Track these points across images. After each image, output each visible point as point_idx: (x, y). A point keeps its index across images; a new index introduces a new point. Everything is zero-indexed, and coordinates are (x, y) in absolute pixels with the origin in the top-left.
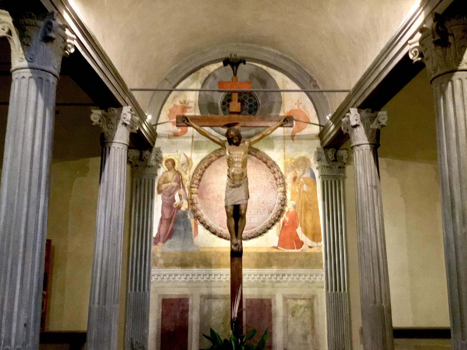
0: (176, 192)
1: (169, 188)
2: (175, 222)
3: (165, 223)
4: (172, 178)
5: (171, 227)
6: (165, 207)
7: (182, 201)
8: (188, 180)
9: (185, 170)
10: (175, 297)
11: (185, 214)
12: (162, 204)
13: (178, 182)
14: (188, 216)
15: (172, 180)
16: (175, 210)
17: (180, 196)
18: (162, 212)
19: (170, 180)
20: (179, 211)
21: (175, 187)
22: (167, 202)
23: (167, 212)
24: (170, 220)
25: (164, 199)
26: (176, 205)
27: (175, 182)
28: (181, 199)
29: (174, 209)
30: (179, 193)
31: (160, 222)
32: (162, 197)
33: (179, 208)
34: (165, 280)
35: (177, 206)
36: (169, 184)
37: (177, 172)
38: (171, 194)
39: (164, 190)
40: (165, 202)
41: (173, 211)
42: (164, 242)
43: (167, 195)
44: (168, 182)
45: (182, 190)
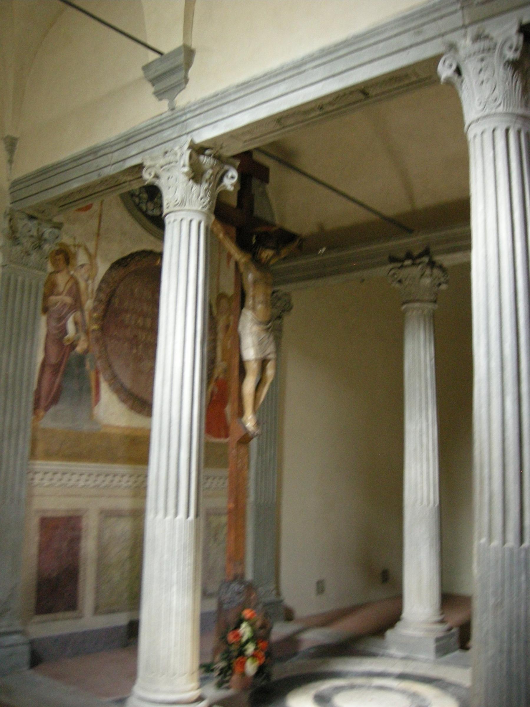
0: (70, 316)
1: (58, 304)
2: (65, 374)
3: (48, 372)
4: (65, 286)
5: (58, 380)
8: (90, 296)
9: (86, 276)
10: (60, 514)
11: (81, 360)
17: (76, 323)
18: (46, 350)
20: (73, 353)
22: (55, 332)
23: (54, 350)
24: (56, 369)
26: (68, 340)
28: (77, 331)
30: (74, 318)
33: (73, 346)
34: (46, 483)
37: (72, 277)
38: (62, 319)
42: (47, 409)
44: (59, 294)
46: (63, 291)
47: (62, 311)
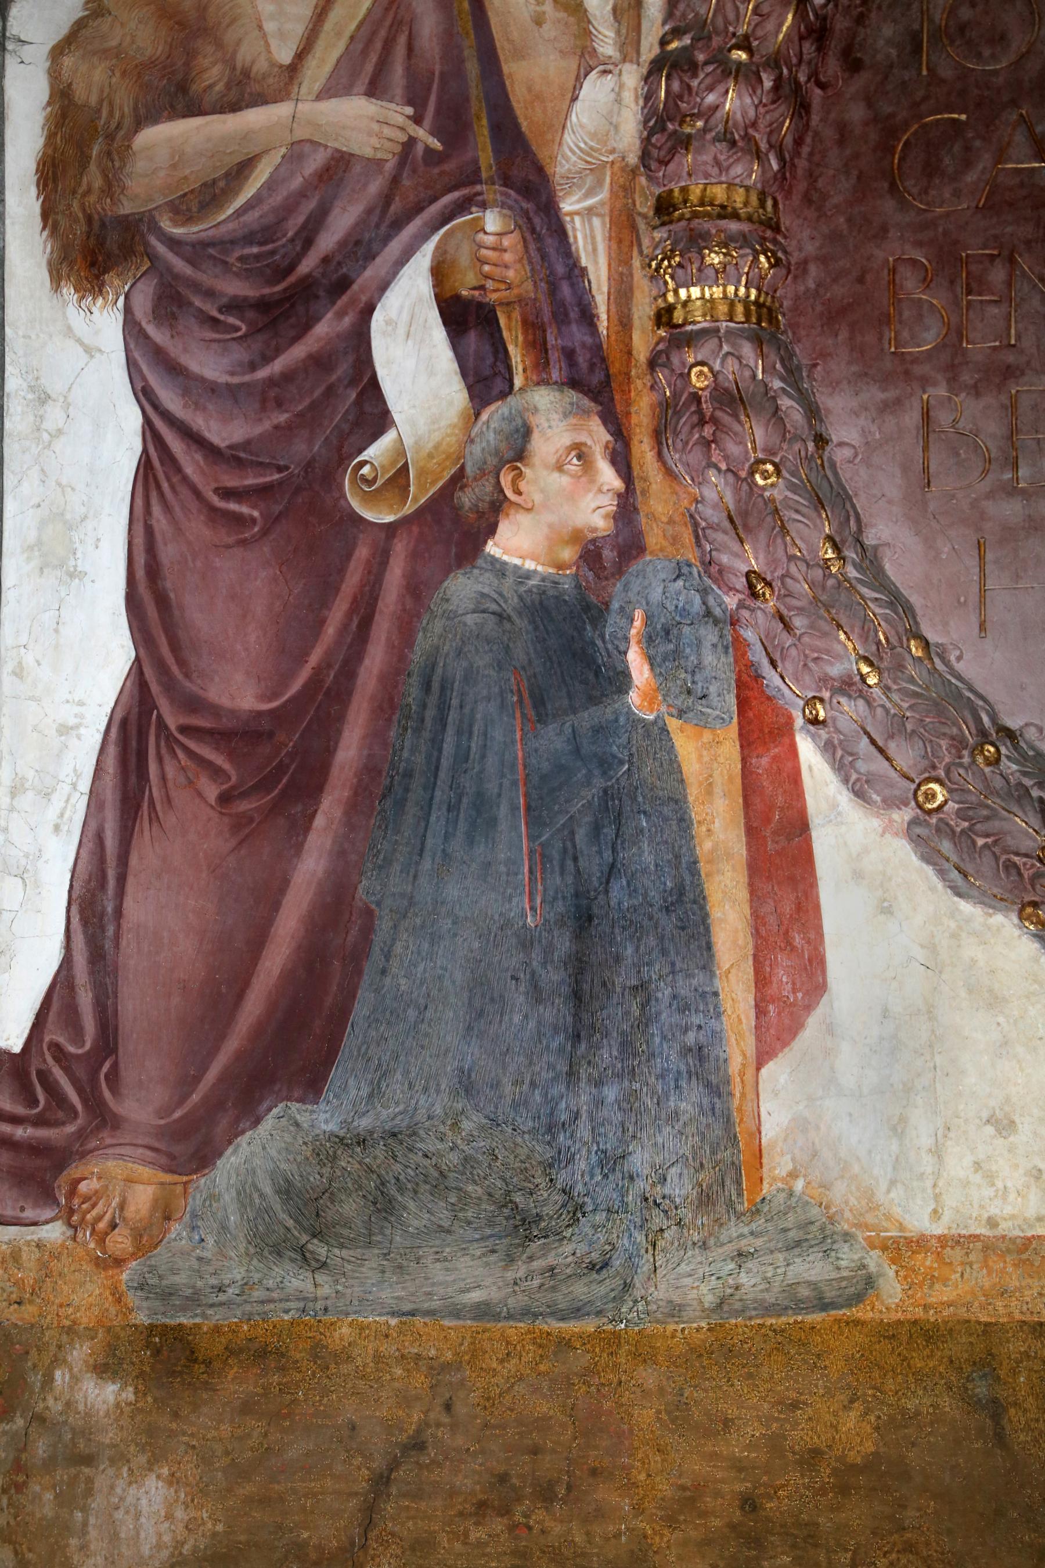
6: (198, 528)
7: (495, 413)
8: (607, 44)
12: (145, 468)
13: (415, 99)
14: (622, 680)
15: (300, 56)
16: (382, 558)
19: (285, 55)
21: (375, 187)
25: (174, 369)
27: (374, 90)
29: (362, 552)
30: (439, 273)
31: (110, 794)
32: (131, 327)
35: (417, 497)
36: (254, 117)
39: (166, 224)
40: (199, 422)
41: (353, 579)
43: (235, 306)
45: (492, 221)
46: (293, 70)
47: (307, 237)
